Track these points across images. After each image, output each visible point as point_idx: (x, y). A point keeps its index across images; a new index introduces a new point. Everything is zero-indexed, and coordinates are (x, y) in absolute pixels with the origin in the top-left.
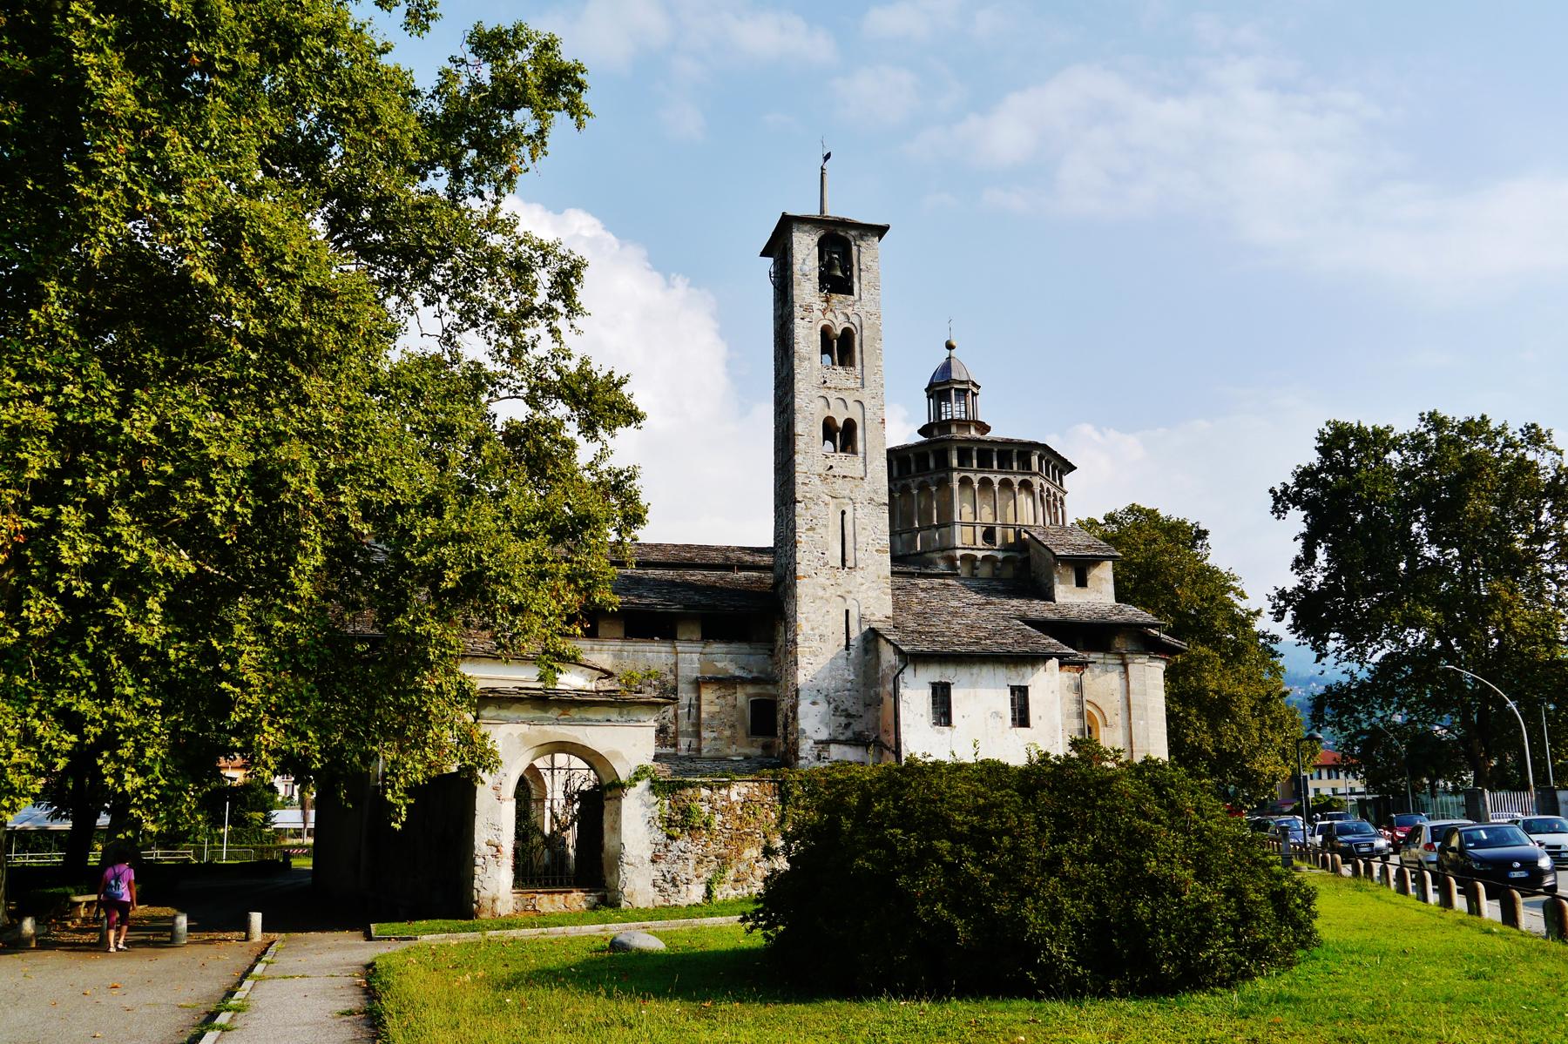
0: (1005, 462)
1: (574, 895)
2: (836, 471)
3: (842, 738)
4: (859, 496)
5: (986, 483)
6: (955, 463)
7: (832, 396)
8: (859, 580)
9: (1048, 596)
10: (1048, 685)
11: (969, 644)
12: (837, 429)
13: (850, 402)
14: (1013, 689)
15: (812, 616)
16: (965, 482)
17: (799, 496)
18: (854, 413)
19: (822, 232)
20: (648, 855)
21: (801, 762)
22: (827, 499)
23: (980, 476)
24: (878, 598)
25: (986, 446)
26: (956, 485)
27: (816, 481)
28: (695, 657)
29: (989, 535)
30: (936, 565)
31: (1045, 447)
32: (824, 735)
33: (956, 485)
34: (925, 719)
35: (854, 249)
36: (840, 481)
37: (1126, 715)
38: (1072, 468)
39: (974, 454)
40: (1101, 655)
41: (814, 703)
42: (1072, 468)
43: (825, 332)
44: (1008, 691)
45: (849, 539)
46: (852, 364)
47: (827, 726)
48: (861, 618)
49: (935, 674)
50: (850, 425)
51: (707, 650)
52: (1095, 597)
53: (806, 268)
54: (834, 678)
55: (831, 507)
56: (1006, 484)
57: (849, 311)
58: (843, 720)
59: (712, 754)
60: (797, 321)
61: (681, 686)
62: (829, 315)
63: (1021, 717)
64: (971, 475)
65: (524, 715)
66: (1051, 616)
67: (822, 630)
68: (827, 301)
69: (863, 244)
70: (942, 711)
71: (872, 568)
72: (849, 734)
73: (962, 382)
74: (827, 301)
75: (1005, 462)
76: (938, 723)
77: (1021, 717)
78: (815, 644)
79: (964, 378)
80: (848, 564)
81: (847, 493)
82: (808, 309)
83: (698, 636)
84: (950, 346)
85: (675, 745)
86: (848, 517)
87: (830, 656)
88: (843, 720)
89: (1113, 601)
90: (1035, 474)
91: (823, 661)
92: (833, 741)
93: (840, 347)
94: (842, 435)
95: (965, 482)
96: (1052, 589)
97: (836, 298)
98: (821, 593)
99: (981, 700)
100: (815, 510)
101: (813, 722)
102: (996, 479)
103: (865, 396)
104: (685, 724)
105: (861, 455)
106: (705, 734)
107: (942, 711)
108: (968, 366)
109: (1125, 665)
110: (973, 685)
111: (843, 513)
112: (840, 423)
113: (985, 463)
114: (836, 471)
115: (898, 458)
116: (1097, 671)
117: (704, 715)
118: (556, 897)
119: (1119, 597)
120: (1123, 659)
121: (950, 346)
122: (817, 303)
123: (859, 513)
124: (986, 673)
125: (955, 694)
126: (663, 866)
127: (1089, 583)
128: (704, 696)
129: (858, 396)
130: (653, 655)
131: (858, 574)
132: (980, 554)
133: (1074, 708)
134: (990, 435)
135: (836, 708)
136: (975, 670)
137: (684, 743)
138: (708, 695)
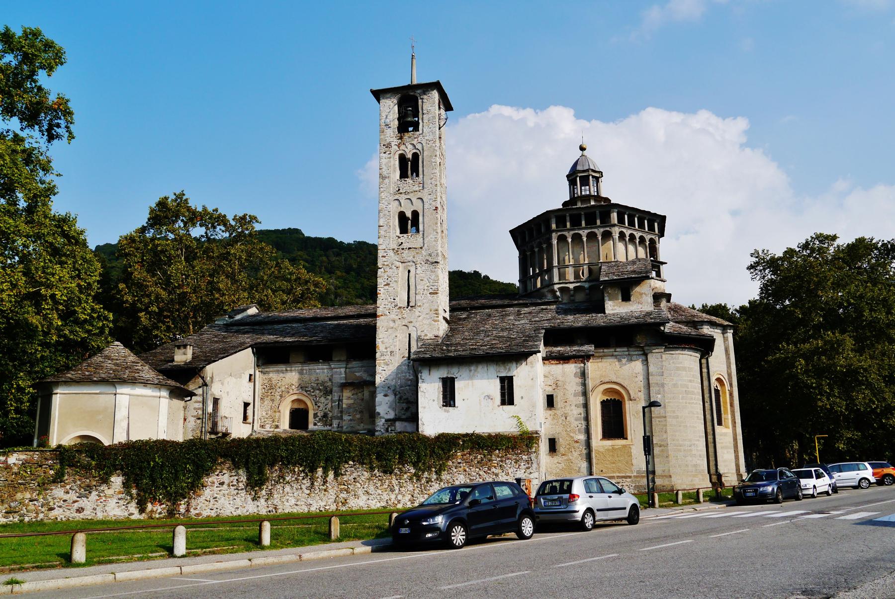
0: (591, 223)
2: (405, 246)
3: (404, 417)
4: (419, 259)
5: (577, 238)
6: (554, 226)
7: (402, 198)
8: (417, 314)
9: (603, 310)
12: (408, 219)
14: (502, 379)
15: (386, 340)
16: (562, 239)
17: (379, 265)
21: (377, 433)
25: (575, 212)
26: (555, 242)
27: (391, 253)
28: (343, 370)
32: (391, 415)
33: (555, 242)
34: (436, 402)
35: (420, 101)
39: (568, 218)
40: (626, 349)
41: (386, 395)
44: (498, 381)
46: (417, 175)
47: (394, 409)
48: (419, 339)
49: (444, 373)
50: (415, 214)
51: (350, 366)
53: (388, 121)
55: (401, 269)
56: (592, 237)
57: (415, 142)
59: (349, 429)
61: (335, 389)
62: (403, 147)
63: (507, 397)
64: (565, 233)
68: (401, 138)
69: (425, 97)
70: (449, 399)
71: (426, 305)
72: (408, 414)
73: (584, 171)
74: (401, 138)
75: (591, 223)
77: (507, 397)
78: (387, 358)
79: (586, 168)
80: (411, 304)
81: (410, 258)
83: (344, 358)
84: (582, 149)
85: (331, 425)
87: (397, 365)
90: (614, 225)
92: (396, 419)
98: (392, 324)
99: (477, 389)
101: (384, 406)
102: (584, 233)
103: (425, 195)
104: (336, 412)
105: (421, 233)
106: (346, 417)
107: (449, 399)
108: (596, 159)
109: (646, 355)
110: (471, 378)
111: (409, 271)
112: (409, 215)
114: (405, 246)
116: (624, 361)
117: (344, 406)
121: (582, 149)
123: (419, 271)
124: (481, 369)
125: (458, 385)
127: (632, 298)
128: (344, 394)
129: (419, 195)
130: (321, 371)
131: (417, 311)
132: (571, 286)
133: (580, 389)
135: (400, 398)
136: (472, 368)
137: (335, 423)
138: (347, 393)
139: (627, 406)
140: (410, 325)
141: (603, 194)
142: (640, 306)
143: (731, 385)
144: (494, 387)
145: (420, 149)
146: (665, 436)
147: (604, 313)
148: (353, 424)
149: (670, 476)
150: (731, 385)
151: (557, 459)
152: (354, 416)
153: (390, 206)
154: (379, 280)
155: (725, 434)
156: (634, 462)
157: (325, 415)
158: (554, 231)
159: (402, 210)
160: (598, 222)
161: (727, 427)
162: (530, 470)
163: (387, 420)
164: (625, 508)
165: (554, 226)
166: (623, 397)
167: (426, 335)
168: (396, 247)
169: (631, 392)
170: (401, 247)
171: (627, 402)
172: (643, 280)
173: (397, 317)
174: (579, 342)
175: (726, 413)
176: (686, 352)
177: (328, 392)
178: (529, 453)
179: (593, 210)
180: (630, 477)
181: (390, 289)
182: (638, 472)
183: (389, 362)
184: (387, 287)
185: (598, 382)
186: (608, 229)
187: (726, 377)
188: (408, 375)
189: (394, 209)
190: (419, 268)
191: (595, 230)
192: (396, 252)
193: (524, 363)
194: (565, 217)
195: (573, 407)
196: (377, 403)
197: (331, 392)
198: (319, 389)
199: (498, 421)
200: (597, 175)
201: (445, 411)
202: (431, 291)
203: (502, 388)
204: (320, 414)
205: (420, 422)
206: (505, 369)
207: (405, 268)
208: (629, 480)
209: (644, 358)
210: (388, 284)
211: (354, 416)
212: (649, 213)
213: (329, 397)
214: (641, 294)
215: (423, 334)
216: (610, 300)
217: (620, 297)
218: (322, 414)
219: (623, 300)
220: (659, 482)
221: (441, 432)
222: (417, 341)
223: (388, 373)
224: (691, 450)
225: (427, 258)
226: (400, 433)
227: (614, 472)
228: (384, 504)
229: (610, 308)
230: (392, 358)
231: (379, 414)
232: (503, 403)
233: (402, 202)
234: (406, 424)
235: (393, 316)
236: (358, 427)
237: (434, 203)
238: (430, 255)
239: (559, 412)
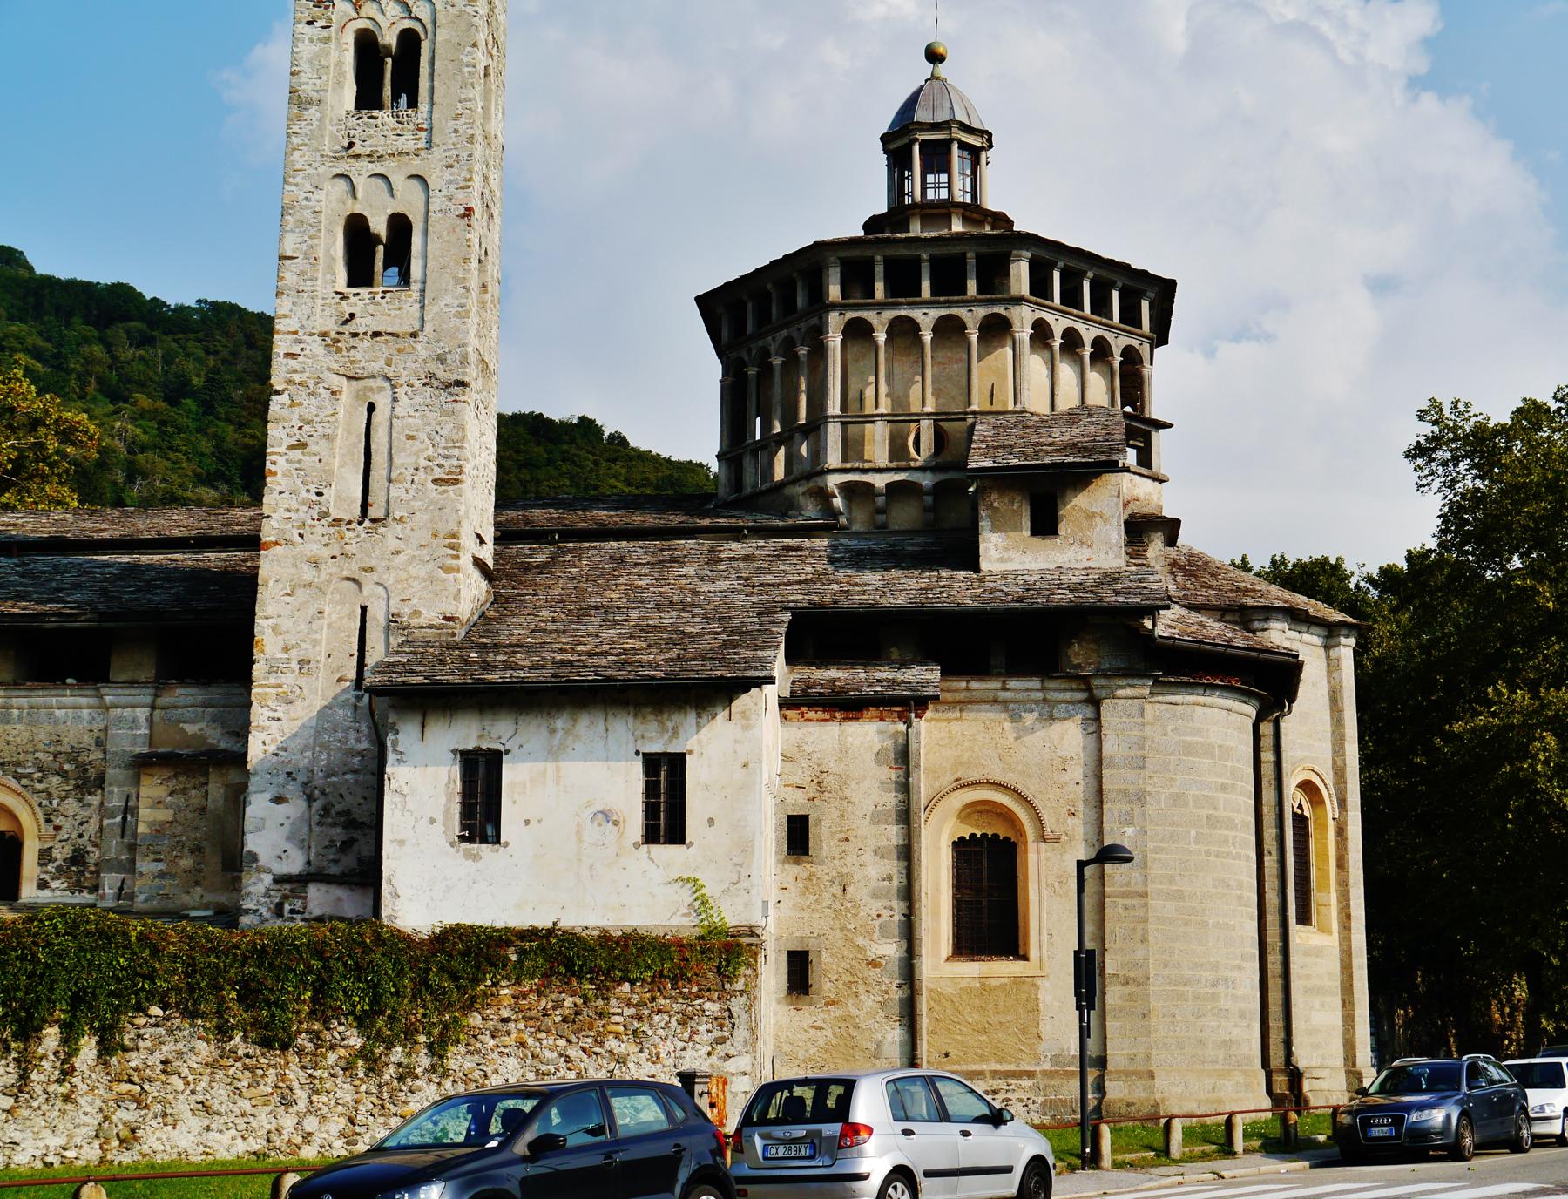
2: (360, 325)
3: (334, 870)
4: (405, 369)
5: (904, 331)
6: (834, 292)
7: (361, 172)
8: (392, 544)
9: (969, 559)
12: (376, 239)
13: (398, 180)
14: (652, 763)
15: (286, 624)
16: (858, 332)
17: (277, 381)
18: (409, 201)
23: (889, 314)
24: (431, 580)
25: (903, 252)
26: (835, 340)
27: (316, 346)
28: (142, 714)
30: (799, 508)
32: (295, 864)
33: (835, 340)
34: (439, 827)
36: (366, 343)
37: (1093, 814)
39: (879, 270)
40: (1035, 683)
41: (278, 800)
43: (367, 45)
44: (638, 767)
45: (379, 459)
46: (413, 103)
47: (304, 846)
48: (393, 622)
49: (467, 732)
50: (400, 226)
51: (165, 700)
54: (325, 747)
56: (949, 329)
58: (338, 834)
61: (111, 773)
63: (666, 819)
64: (869, 315)
67: (306, 650)
70: (480, 815)
71: (422, 518)
72: (349, 861)
73: (935, 127)
75: (949, 286)
77: (666, 819)
78: (289, 679)
79: (942, 116)
80: (372, 513)
81: (378, 366)
84: (934, 56)
85: (95, 889)
86: (380, 416)
87: (319, 703)
88: (338, 834)
90: (1019, 300)
91: (304, 712)
95: (858, 332)
98: (308, 574)
99: (573, 783)
100: (309, 406)
101: (273, 835)
102: (926, 318)
104: (114, 847)
105: (415, 287)
106: (145, 866)
107: (480, 815)
108: (975, 93)
109: (1095, 703)
110: (554, 754)
111: (371, 408)
112: (379, 226)
114: (360, 325)
116: (1029, 718)
117: (142, 829)
120: (1089, 690)
121: (934, 56)
124: (588, 727)
125: (510, 774)
127: (1063, 528)
128: (144, 792)
129: (416, 166)
131: (391, 533)
132: (880, 481)
133: (891, 800)
135: (326, 810)
136: (560, 723)
138: (153, 789)
139: (1032, 857)
140: (368, 580)
141: (991, 203)
142: (1086, 552)
143: (1342, 803)
144: (626, 788)
145: (426, 19)
146: (1140, 953)
147: (977, 569)
148: (169, 886)
149: (1152, 1075)
150: (1342, 803)
151: (809, 1015)
152: (173, 862)
153: (319, 195)
154: (274, 431)
155: (1318, 952)
156: (1046, 1028)
157: (78, 858)
159: (357, 210)
160: (972, 287)
161: (1324, 930)
162: (727, 1048)
163: (279, 880)
164: (1009, 1170)
165: (834, 292)
166: (1021, 832)
167: (417, 613)
168: (331, 327)
169: (1045, 815)
170: (350, 327)
171: (1032, 846)
172: (1098, 475)
173: (326, 553)
174: (895, 654)
175: (1324, 887)
176: (1216, 699)
177: (88, 782)
178: (725, 995)
179: (957, 250)
180: (1030, 1075)
181: (309, 461)
182: (1055, 1059)
183: (293, 696)
185: (947, 781)
186: (999, 309)
187: (1330, 780)
188: (352, 736)
189: (333, 206)
190: (404, 400)
191: (961, 312)
192: (332, 342)
193: (722, 715)
194: (869, 264)
195: (868, 857)
196: (248, 825)
197: (100, 782)
198: (61, 773)
199: (639, 894)
200: (976, 141)
201: (468, 855)
202: (438, 473)
203: (651, 789)
204: (61, 853)
205: (385, 889)
206: (664, 730)
207: (358, 396)
208: (1026, 1083)
209: (1089, 711)
210: (301, 445)
211: (173, 862)
212: (1125, 268)
213: (94, 800)
214: (1091, 516)
215: (406, 610)
216: (995, 528)
217: (1026, 523)
218: (68, 851)
219: (1034, 533)
220: (1116, 1090)
221: (451, 920)
222: (387, 630)
223: (290, 727)
224: (1215, 997)
225: (433, 367)
226: (320, 919)
227: (983, 1059)
228: (256, 1145)
229: (994, 554)
230: (302, 681)
231: (254, 857)
232: (651, 836)
233: (361, 183)
234: (339, 892)
235: (313, 547)
236: (186, 899)
237: (460, 195)
238: (441, 359)
239: (823, 871)
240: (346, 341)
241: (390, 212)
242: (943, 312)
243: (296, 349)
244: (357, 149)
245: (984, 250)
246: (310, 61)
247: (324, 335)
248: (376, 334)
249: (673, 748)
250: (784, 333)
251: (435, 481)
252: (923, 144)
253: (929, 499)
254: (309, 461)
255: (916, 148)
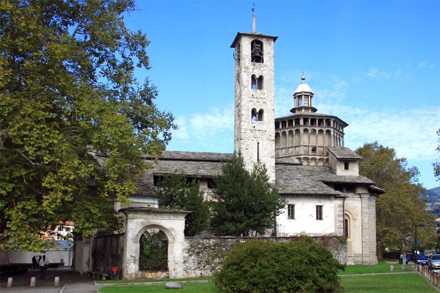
1: (159, 273)
10: (330, 208)
11: (302, 191)
14: (317, 206)
16: (306, 131)
18: (264, 107)
19: (252, 40)
20: (182, 261)
22: (253, 138)
27: (249, 131)
29: (314, 150)
31: (336, 117)
34: (285, 217)
38: (347, 125)
39: (310, 121)
42: (347, 125)
43: (253, 77)
44: (316, 207)
50: (261, 112)
52: (353, 173)
55: (255, 141)
56: (321, 131)
60: (243, 73)
63: (319, 216)
65: (142, 216)
66: (334, 180)
70: (291, 215)
76: (289, 218)
77: (319, 216)
81: (260, 136)
82: (247, 68)
89: (358, 175)
93: (258, 81)
94: (258, 114)
96: (335, 170)
97: (258, 64)
102: (317, 129)
107: (291, 215)
111: (258, 143)
113: (313, 122)
115: (278, 123)
118: (153, 273)
119: (361, 171)
122: (251, 67)
125: (296, 208)
126: (187, 265)
129: (265, 101)
132: (310, 157)
134: (318, 113)
142: (353, 173)
147: (336, 174)
158: (302, 126)
159: (255, 108)
180: (351, 257)
181: (249, 152)
182: (354, 254)
184: (246, 151)
192: (252, 131)
202: (271, 156)
210: (247, 149)
229: (339, 172)
238: (270, 136)
240: (254, 131)
241: (260, 108)
242: (320, 128)
243: (245, 132)
244: (254, 96)
245: (327, 118)
246: (245, 79)
247: (250, 130)
248: (259, 130)
249: (321, 205)
250: (290, 129)
251: (270, 157)
252: (304, 95)
253: (325, 161)
254: (249, 152)
255: (303, 96)
